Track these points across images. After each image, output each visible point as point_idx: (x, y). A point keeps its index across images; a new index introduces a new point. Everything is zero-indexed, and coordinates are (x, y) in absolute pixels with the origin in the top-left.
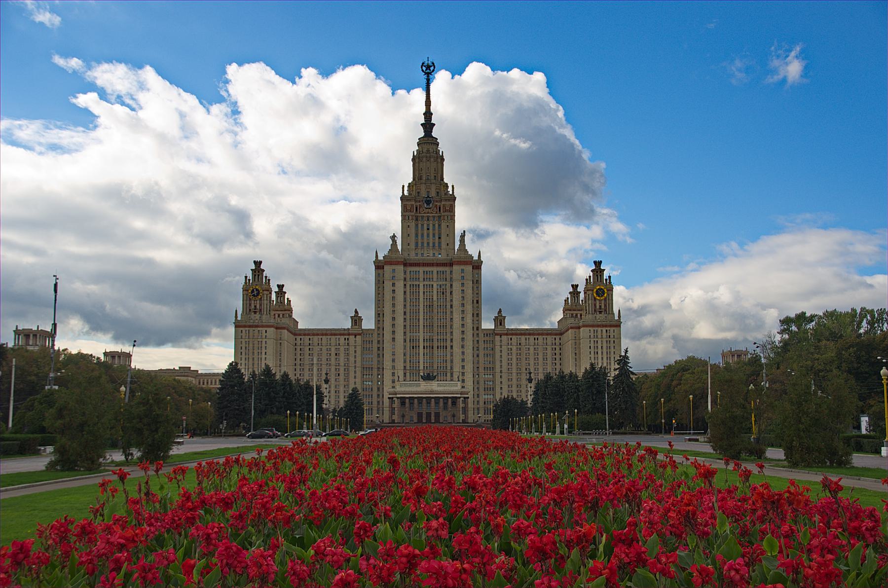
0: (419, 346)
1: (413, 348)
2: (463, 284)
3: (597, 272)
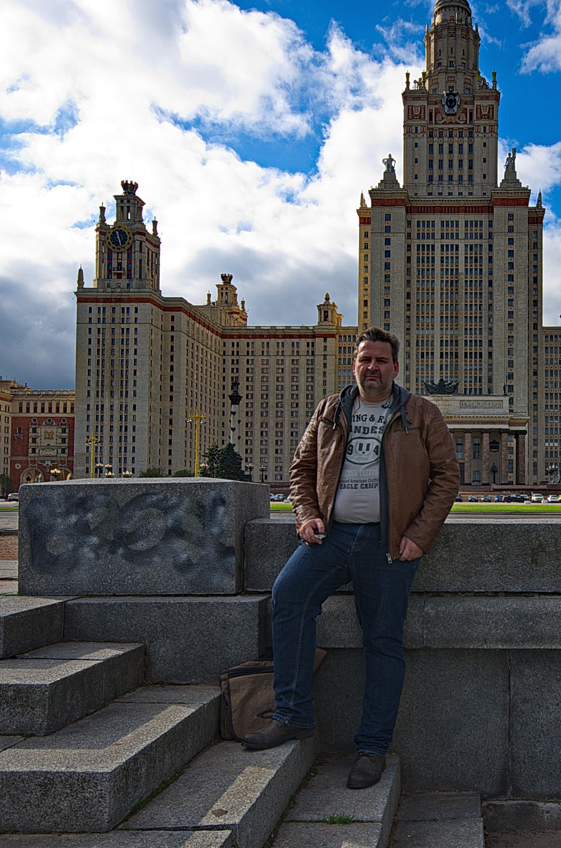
0: (432, 354)
1: (423, 357)
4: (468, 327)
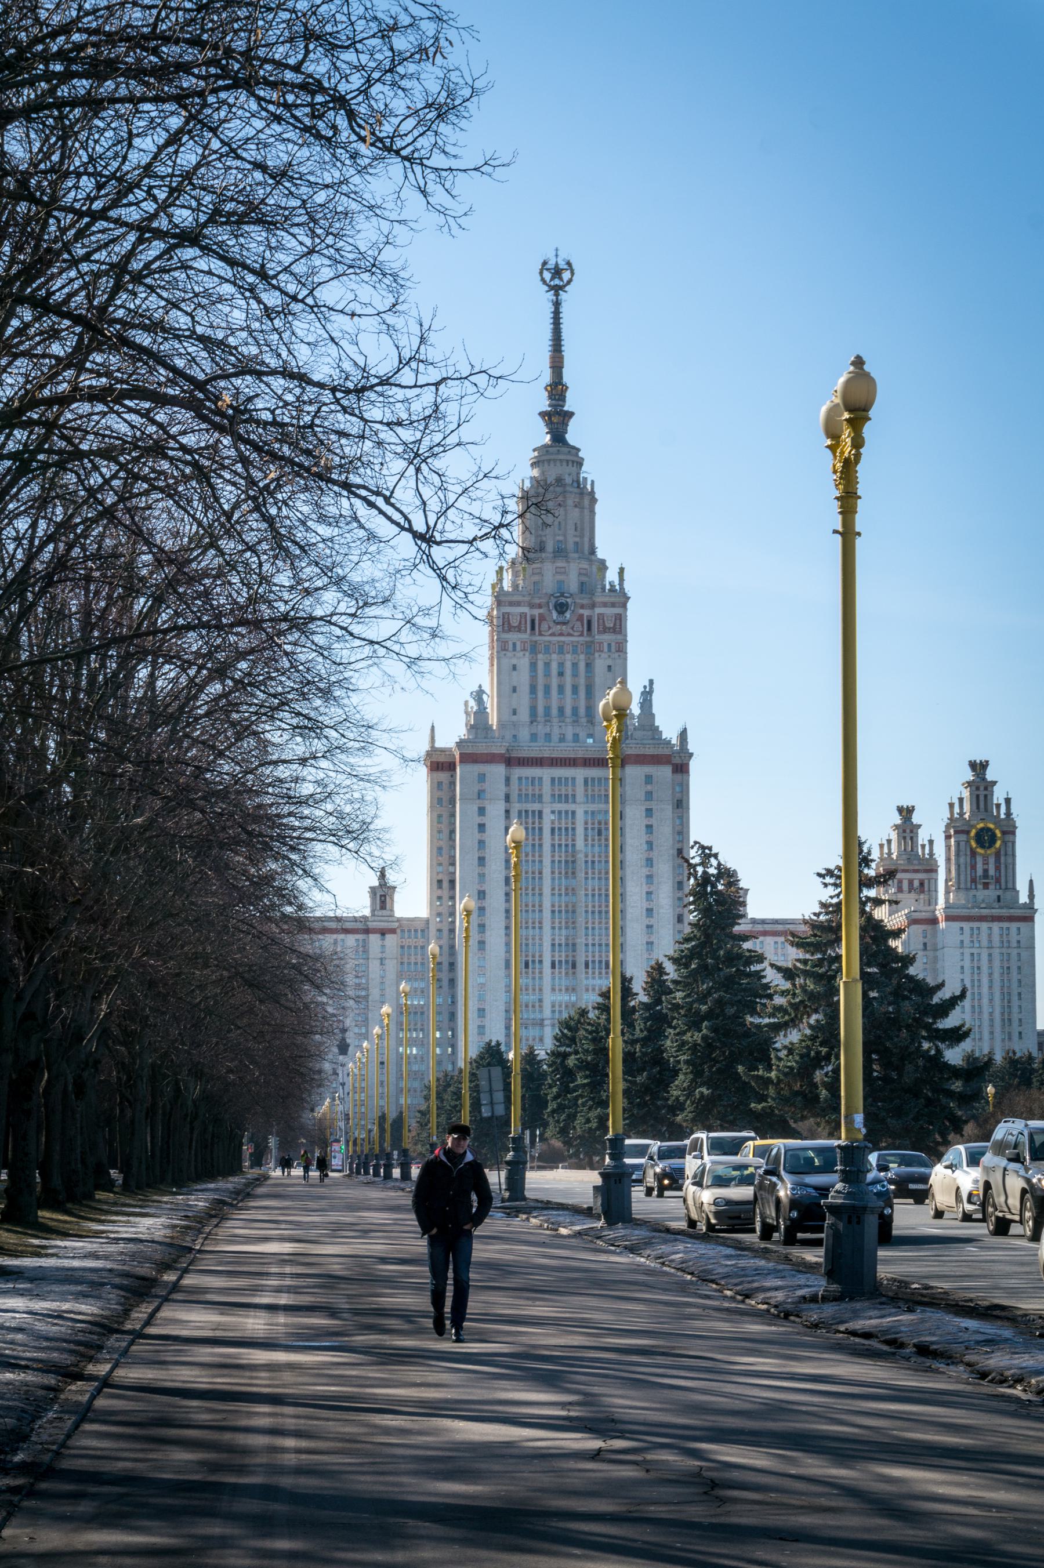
0: (541, 962)
1: (527, 966)
2: (649, 812)
3: (978, 789)
4: (590, 926)
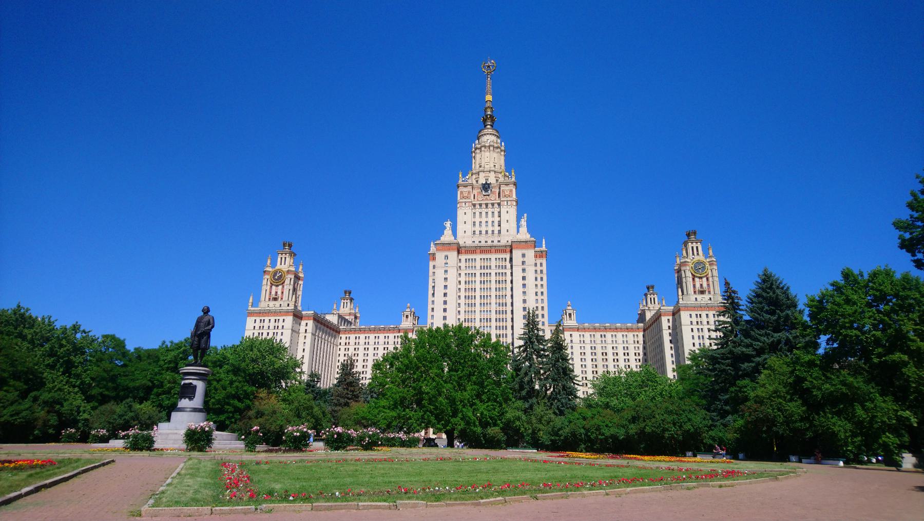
2: (524, 270)
